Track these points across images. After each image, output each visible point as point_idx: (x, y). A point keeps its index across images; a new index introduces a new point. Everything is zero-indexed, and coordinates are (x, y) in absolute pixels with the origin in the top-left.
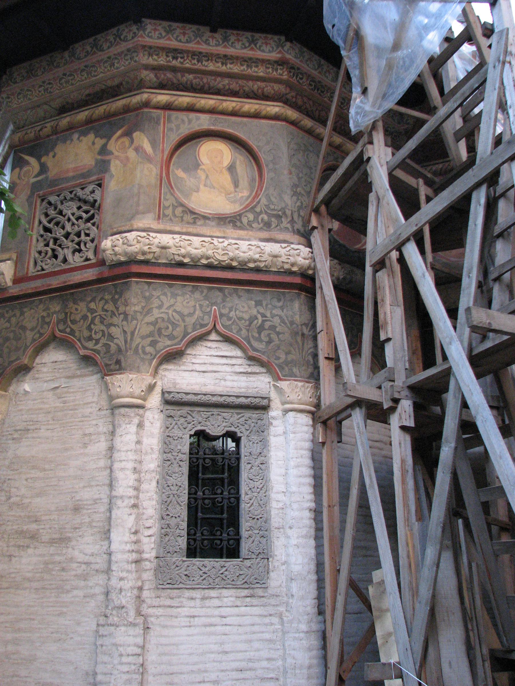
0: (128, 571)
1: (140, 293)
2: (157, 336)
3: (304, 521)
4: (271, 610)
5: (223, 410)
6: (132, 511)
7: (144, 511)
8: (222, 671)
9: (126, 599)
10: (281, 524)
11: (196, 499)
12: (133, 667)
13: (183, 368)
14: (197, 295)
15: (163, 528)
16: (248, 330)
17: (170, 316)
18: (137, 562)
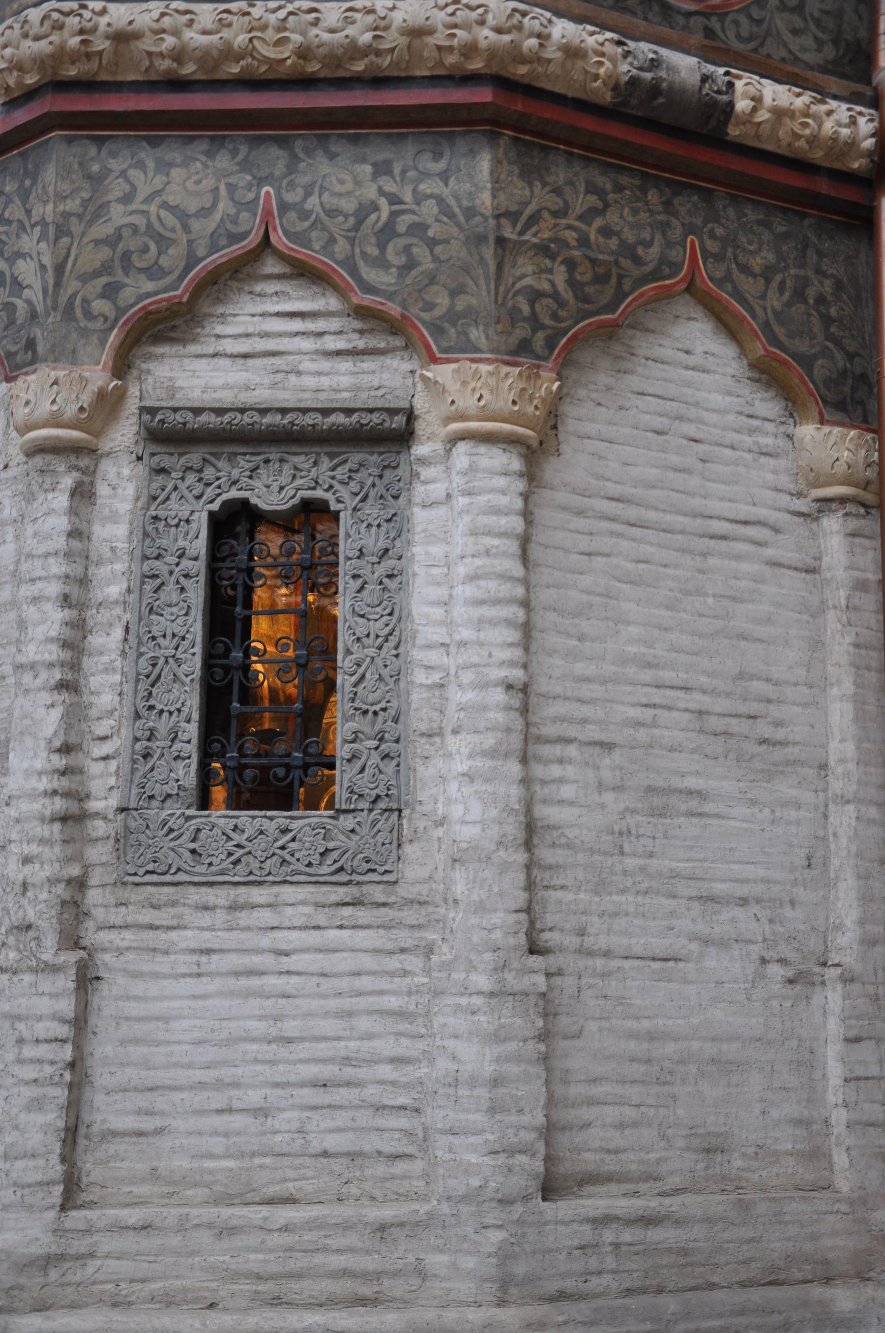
0: (42, 841)
1: (76, 167)
2: (120, 272)
3: (491, 715)
4: (405, 937)
5: (294, 449)
6: (58, 698)
7: (93, 699)
8: (277, 1085)
9: (40, 909)
10: (435, 725)
11: (227, 670)
12: (48, 1070)
13: (193, 348)
14: (223, 161)
15: (137, 740)
16: (352, 241)
17: (153, 219)
18: (64, 819)
